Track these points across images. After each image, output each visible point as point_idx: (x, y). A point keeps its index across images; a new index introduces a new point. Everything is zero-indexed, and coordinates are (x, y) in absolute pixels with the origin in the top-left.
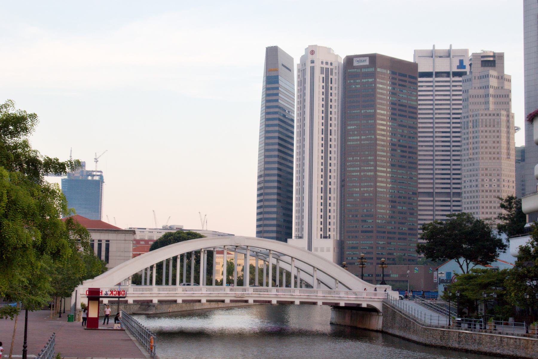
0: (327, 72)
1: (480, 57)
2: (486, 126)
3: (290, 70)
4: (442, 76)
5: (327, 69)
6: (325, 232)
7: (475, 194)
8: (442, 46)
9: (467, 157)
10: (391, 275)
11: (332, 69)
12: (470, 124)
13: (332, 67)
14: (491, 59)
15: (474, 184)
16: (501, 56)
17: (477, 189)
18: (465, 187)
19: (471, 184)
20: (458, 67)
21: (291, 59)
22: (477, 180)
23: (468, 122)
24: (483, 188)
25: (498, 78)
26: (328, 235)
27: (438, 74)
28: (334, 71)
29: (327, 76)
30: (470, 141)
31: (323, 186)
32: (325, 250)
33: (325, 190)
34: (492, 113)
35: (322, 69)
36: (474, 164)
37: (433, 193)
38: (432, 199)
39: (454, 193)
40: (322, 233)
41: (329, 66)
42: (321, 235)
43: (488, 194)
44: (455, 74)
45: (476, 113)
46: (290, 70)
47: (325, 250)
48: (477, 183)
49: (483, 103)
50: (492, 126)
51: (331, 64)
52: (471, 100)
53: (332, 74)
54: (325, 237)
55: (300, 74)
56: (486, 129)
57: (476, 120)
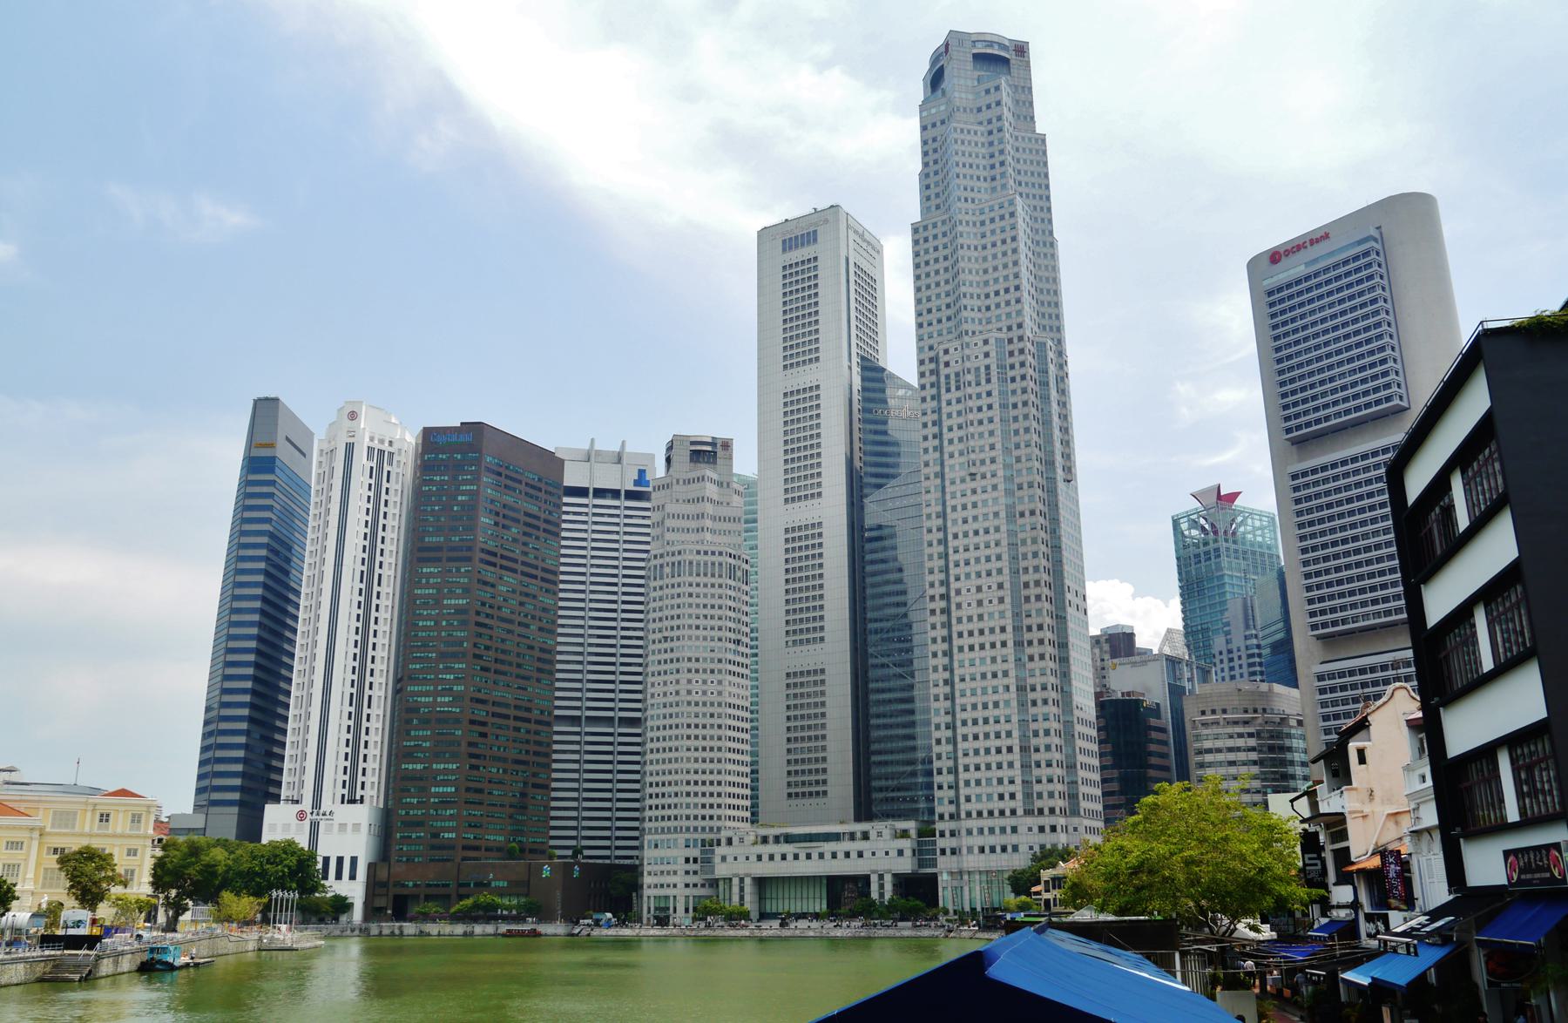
0: (381, 457)
2: (698, 575)
3: (304, 455)
4: (604, 497)
5: (381, 452)
6: (353, 790)
7: (674, 710)
8: (608, 444)
9: (658, 636)
10: (493, 884)
11: (391, 454)
12: (667, 570)
13: (391, 450)
14: (709, 448)
15: (671, 688)
16: (727, 445)
17: (677, 699)
18: (653, 696)
19: (665, 689)
20: (637, 483)
21: (310, 435)
22: (678, 682)
23: (662, 566)
25: (720, 484)
26: (358, 797)
27: (599, 493)
28: (396, 458)
30: (667, 602)
31: (354, 691)
32: (350, 828)
33: (358, 700)
34: (710, 549)
36: (659, 662)
37: (579, 718)
38: (577, 729)
39: (620, 718)
40: (345, 792)
41: (386, 447)
42: (343, 796)
43: (700, 709)
44: (631, 495)
45: (679, 548)
46: (304, 455)
47: (350, 828)
48: (677, 687)
51: (391, 443)
52: (669, 523)
53: (390, 463)
54: (352, 801)
55: (323, 459)
56: (698, 579)
57: (679, 563)
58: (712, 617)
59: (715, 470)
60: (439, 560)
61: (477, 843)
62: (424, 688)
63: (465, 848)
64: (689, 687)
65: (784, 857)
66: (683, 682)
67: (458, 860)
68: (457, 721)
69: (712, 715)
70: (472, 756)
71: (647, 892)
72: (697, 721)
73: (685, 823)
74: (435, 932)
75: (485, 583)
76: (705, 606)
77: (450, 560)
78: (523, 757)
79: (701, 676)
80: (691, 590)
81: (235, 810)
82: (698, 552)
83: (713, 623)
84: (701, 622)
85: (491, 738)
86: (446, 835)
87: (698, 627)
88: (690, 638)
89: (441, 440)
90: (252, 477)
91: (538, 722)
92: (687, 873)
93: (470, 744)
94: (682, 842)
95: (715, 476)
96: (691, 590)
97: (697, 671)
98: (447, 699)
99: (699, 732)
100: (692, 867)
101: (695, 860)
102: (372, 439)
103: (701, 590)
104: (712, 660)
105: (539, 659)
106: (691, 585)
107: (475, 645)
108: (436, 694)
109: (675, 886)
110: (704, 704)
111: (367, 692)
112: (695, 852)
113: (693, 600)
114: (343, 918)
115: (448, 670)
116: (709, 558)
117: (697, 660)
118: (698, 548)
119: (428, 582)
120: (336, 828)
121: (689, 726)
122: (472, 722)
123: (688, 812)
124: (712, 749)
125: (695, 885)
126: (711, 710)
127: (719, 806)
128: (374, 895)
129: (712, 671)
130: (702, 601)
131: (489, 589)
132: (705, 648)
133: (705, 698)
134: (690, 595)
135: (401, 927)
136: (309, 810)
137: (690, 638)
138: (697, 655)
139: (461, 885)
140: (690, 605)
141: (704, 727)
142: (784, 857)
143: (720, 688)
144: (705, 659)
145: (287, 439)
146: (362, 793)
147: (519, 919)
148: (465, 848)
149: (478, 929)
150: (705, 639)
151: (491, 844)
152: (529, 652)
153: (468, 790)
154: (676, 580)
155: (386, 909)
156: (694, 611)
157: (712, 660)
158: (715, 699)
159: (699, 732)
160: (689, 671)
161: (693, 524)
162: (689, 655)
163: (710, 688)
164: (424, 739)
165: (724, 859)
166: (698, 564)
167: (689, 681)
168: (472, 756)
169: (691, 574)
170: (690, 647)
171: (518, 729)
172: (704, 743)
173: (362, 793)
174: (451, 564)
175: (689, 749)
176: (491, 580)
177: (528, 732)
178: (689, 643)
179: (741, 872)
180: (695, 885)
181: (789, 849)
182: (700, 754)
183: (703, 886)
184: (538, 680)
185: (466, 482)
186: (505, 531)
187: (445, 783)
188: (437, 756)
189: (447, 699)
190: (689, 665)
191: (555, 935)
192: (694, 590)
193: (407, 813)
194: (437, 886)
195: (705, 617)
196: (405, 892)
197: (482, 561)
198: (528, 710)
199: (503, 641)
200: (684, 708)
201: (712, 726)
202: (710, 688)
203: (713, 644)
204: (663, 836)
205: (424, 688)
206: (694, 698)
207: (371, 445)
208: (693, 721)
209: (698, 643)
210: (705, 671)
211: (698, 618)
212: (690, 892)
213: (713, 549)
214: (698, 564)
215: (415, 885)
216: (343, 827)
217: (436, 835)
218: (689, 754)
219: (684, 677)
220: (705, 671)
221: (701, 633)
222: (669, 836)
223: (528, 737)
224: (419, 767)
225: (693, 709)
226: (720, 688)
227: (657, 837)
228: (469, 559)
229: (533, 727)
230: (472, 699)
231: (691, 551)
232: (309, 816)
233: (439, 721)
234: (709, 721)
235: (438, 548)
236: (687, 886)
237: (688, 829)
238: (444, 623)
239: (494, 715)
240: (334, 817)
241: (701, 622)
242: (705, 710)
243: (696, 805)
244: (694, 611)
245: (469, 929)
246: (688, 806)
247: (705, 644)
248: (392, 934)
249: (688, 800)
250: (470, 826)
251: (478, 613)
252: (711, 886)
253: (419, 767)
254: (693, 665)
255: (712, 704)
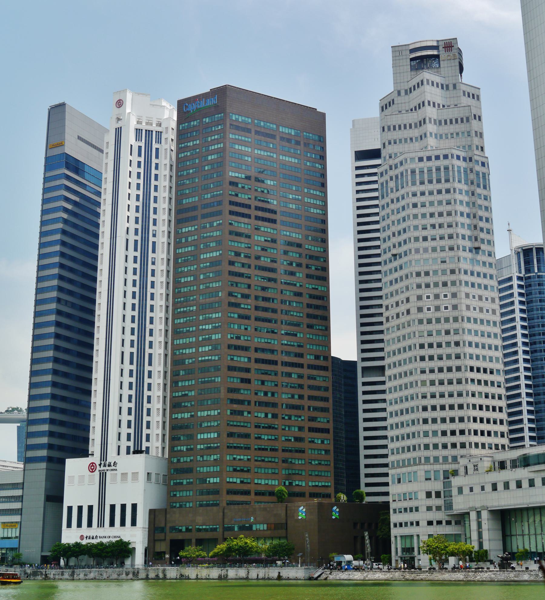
1: (408, 52)
2: (422, 183)
5: (149, 133)
10: (254, 528)
11: (159, 134)
12: (392, 184)
13: (159, 129)
15: (403, 308)
24: (420, 316)
25: (444, 87)
26: (144, 449)
28: (164, 136)
29: (148, 145)
32: (130, 476)
34: (433, 154)
35: (138, 131)
40: (131, 444)
41: (154, 128)
43: (433, 327)
47: (130, 476)
49: (416, 138)
50: (435, 181)
51: (159, 125)
53: (159, 141)
56: (422, 188)
58: (441, 226)
59: (438, 73)
60: (195, 218)
61: (245, 487)
62: (188, 340)
63: (229, 492)
64: (420, 304)
65: (519, 485)
66: (413, 299)
67: (224, 504)
68: (217, 369)
69: (447, 332)
70: (233, 401)
71: (394, 532)
72: (430, 340)
73: (423, 453)
74: (193, 576)
75: (238, 234)
76: (432, 215)
77: (204, 216)
78: (296, 401)
79: (432, 291)
80: (415, 200)
81: (44, 465)
82: (421, 159)
83: (441, 231)
84: (430, 232)
85: (255, 384)
86: (212, 480)
87: (425, 239)
88: (417, 251)
89: (192, 108)
90: (49, 174)
91: (310, 367)
92: (429, 509)
93: (231, 390)
94: (421, 474)
95: (437, 79)
96: (415, 200)
97: (428, 286)
98: (207, 349)
99: (434, 352)
100: (434, 502)
101: (438, 494)
102: (138, 122)
103: (426, 199)
104: (444, 272)
105: (309, 306)
106: (414, 195)
107: (230, 294)
108: (198, 344)
109: (418, 523)
110: (438, 321)
111: (148, 351)
112: (437, 486)
113: (419, 211)
114: (128, 562)
115: (207, 321)
116: (434, 164)
117: (427, 274)
118: (421, 154)
119: (187, 241)
120: (119, 477)
121: (422, 346)
122: (230, 368)
123: (426, 441)
124: (450, 369)
125: (439, 523)
126: (447, 326)
127: (462, 432)
128: (155, 541)
129: (445, 284)
130: (428, 210)
131: (243, 239)
132: (435, 259)
133: (438, 315)
134: (415, 205)
135: (164, 571)
136: (98, 463)
137: (417, 251)
138: (426, 268)
139: (225, 529)
140: (415, 216)
141: (439, 345)
142: (519, 485)
143: (454, 301)
144: (435, 272)
145: (79, 138)
146: (148, 444)
147: (268, 562)
148: (229, 492)
149: (232, 573)
150: (434, 250)
151: (263, 489)
152: (297, 299)
153: (231, 435)
154: (402, 192)
155: (164, 553)
156: (420, 222)
157: (444, 272)
158: (450, 313)
159: (434, 352)
160: (419, 286)
161: (415, 133)
162: (417, 269)
163: (443, 302)
164: (190, 389)
165: (460, 490)
166: (422, 172)
167: (419, 298)
168: (233, 401)
169: (414, 184)
170: (417, 261)
171: (289, 375)
172: (441, 364)
173: (148, 444)
174: (205, 220)
175: (423, 372)
176: (246, 232)
177: (300, 376)
178: (417, 257)
179: (478, 505)
180: (439, 523)
181: (523, 474)
182: (437, 376)
183: (448, 523)
184: (310, 326)
185: (214, 142)
186: (259, 184)
187: (209, 430)
188: (201, 404)
189: (207, 349)
190: (418, 280)
191: (296, 579)
192: (418, 200)
193: (179, 461)
194: (206, 530)
195: (433, 226)
196: (180, 537)
197: (231, 213)
198: (301, 355)
199: (264, 289)
200: (416, 328)
201: (448, 344)
202: (443, 302)
203: (443, 254)
204: (404, 470)
205: (188, 340)
206: (426, 315)
207: (139, 127)
208: (427, 340)
209: (426, 256)
210: (436, 285)
211: (425, 228)
212: (435, 530)
213: (437, 153)
214: (422, 172)
215: (188, 530)
216: (124, 475)
217: (204, 481)
218: (424, 377)
219: (413, 294)
220: (436, 285)
221: (430, 244)
222: (409, 469)
223: (301, 381)
224: (187, 415)
225: (426, 327)
226: (454, 301)
227: (399, 471)
228: (219, 213)
229: (306, 372)
230: (229, 347)
231: (412, 159)
232: (98, 467)
233: (204, 370)
234: (444, 339)
235: (194, 208)
236: (430, 523)
237: (427, 459)
238: (202, 277)
239: (257, 361)
240: (117, 467)
241: (430, 232)
242: (439, 327)
243: (435, 433)
244: (420, 222)
245: (223, 572)
246: (426, 434)
247: (435, 255)
248: (157, 577)
249: (426, 427)
250: (235, 470)
251: (232, 263)
252: (457, 523)
253: (187, 415)
254: (423, 280)
255: (447, 320)
